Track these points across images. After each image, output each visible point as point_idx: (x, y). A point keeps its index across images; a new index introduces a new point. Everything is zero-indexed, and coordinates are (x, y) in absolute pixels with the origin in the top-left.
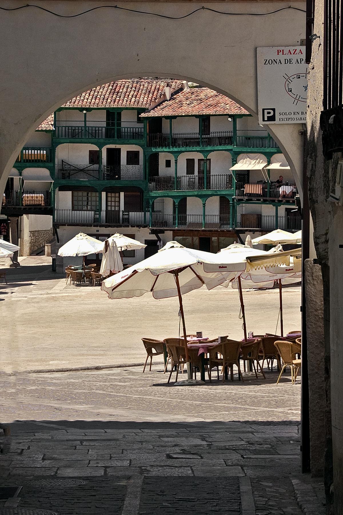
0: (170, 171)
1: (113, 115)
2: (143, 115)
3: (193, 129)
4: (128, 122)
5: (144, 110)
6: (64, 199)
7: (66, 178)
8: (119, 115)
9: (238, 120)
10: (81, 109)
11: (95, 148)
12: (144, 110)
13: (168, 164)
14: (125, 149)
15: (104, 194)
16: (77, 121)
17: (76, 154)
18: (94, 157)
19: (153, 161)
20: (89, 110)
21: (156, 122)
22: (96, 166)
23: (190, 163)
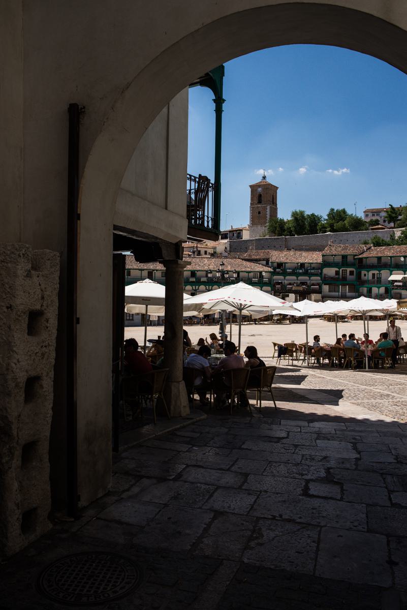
0: (366, 278)
1: (344, 257)
2: (356, 257)
3: (375, 261)
4: (350, 259)
5: (356, 255)
6: (326, 288)
7: (326, 280)
8: (347, 257)
9: (392, 258)
10: (332, 255)
11: (338, 269)
12: (356, 255)
13: (365, 275)
14: (349, 270)
15: (340, 286)
16: (331, 259)
17: (330, 272)
18: (337, 273)
19: (359, 274)
20: (335, 255)
21: (361, 260)
22: (337, 276)
23: (374, 275)
